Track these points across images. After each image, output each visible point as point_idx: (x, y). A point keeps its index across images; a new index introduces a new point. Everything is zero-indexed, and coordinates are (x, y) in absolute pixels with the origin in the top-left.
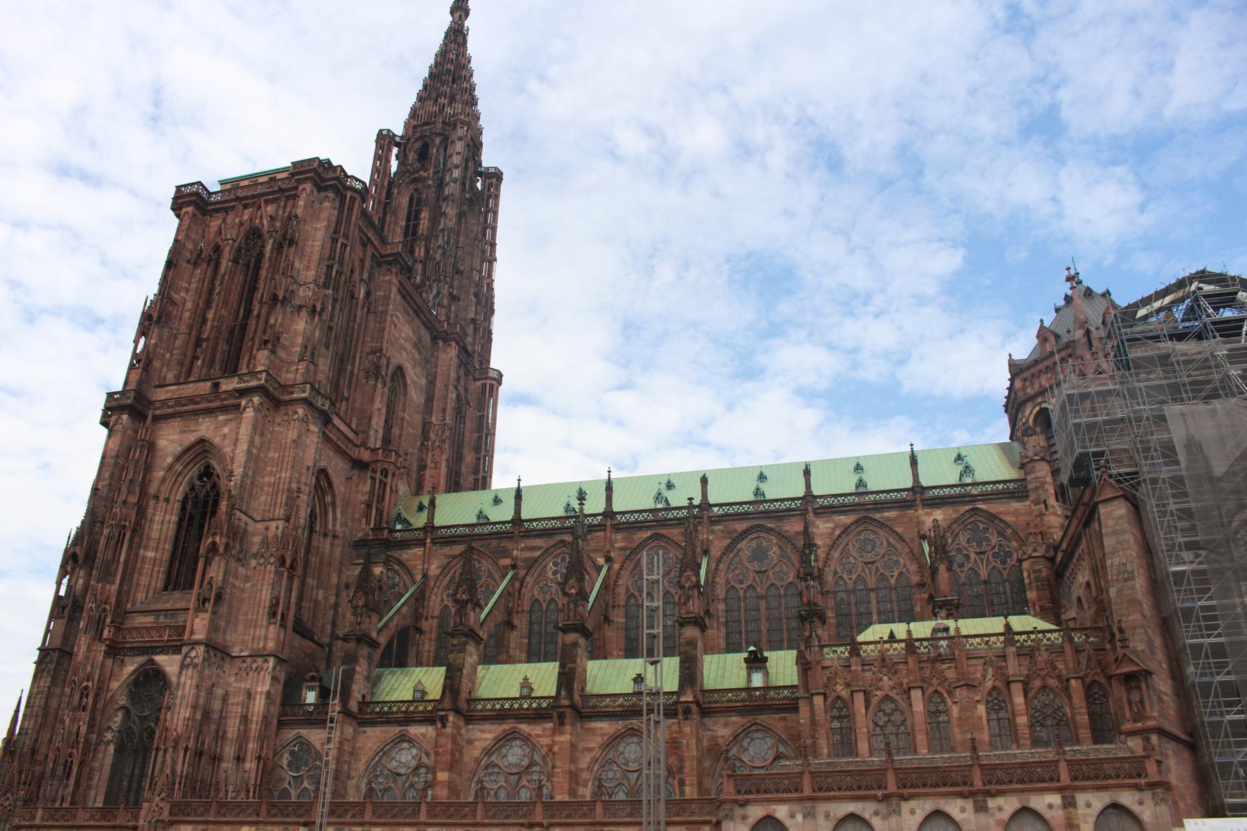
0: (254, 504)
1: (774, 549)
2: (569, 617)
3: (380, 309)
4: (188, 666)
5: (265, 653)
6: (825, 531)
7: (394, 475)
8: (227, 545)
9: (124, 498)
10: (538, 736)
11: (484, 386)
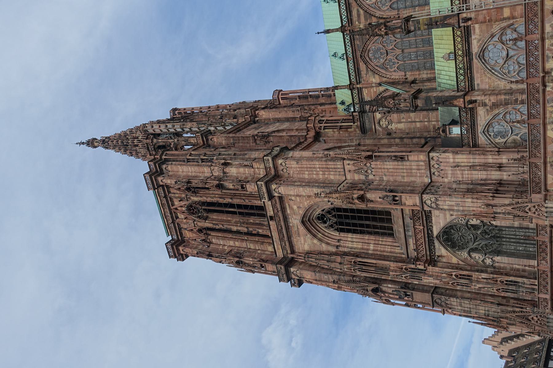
3: (232, 141)
4: (437, 205)
5: (427, 159)
7: (322, 117)
8: (358, 190)
9: (338, 264)
11: (282, 99)
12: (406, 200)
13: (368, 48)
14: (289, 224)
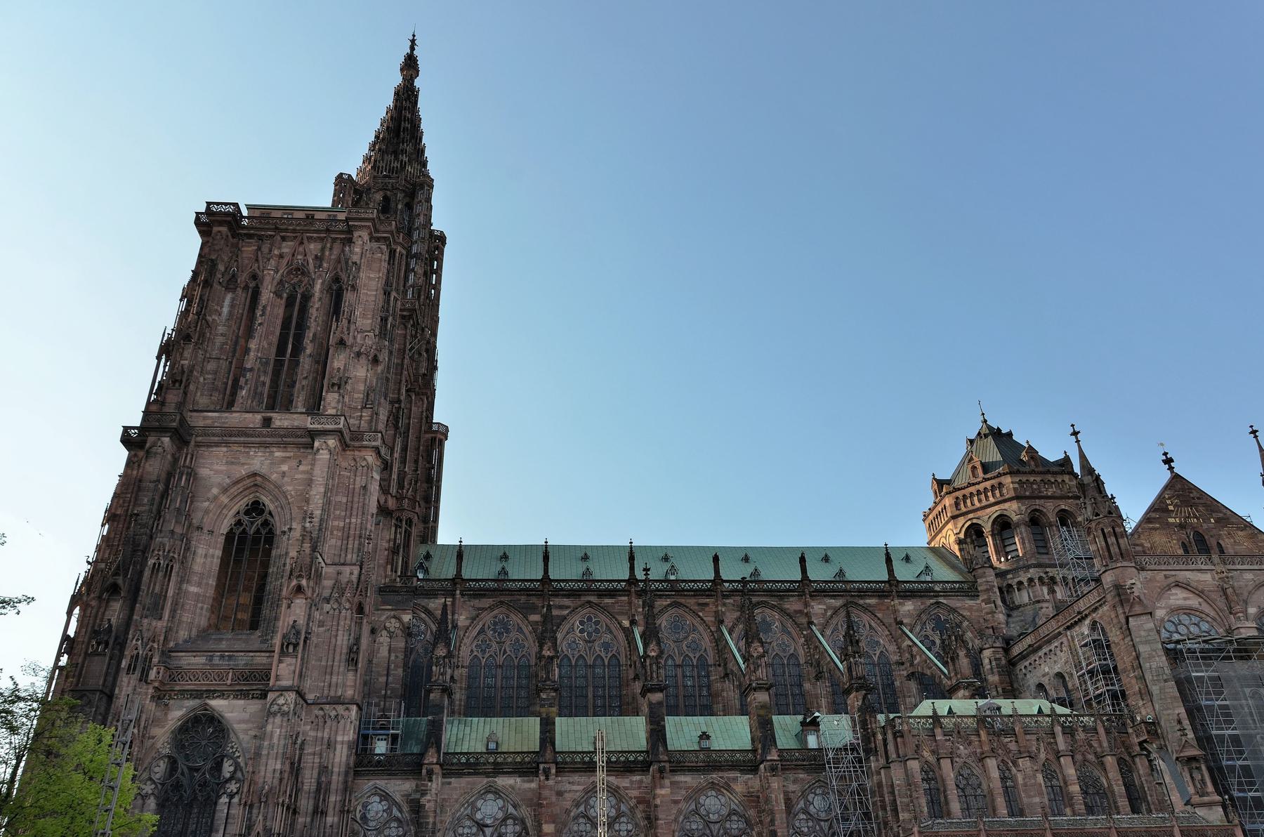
0: (326, 549)
1: (777, 623)
2: (652, 678)
4: (275, 714)
5: (346, 701)
6: (820, 611)
10: (626, 788)
11: (433, 439)
12: (288, 665)
13: (512, 615)
14: (253, 449)
